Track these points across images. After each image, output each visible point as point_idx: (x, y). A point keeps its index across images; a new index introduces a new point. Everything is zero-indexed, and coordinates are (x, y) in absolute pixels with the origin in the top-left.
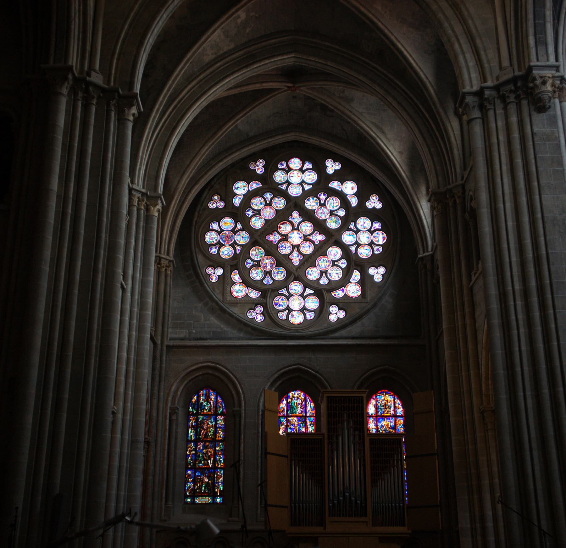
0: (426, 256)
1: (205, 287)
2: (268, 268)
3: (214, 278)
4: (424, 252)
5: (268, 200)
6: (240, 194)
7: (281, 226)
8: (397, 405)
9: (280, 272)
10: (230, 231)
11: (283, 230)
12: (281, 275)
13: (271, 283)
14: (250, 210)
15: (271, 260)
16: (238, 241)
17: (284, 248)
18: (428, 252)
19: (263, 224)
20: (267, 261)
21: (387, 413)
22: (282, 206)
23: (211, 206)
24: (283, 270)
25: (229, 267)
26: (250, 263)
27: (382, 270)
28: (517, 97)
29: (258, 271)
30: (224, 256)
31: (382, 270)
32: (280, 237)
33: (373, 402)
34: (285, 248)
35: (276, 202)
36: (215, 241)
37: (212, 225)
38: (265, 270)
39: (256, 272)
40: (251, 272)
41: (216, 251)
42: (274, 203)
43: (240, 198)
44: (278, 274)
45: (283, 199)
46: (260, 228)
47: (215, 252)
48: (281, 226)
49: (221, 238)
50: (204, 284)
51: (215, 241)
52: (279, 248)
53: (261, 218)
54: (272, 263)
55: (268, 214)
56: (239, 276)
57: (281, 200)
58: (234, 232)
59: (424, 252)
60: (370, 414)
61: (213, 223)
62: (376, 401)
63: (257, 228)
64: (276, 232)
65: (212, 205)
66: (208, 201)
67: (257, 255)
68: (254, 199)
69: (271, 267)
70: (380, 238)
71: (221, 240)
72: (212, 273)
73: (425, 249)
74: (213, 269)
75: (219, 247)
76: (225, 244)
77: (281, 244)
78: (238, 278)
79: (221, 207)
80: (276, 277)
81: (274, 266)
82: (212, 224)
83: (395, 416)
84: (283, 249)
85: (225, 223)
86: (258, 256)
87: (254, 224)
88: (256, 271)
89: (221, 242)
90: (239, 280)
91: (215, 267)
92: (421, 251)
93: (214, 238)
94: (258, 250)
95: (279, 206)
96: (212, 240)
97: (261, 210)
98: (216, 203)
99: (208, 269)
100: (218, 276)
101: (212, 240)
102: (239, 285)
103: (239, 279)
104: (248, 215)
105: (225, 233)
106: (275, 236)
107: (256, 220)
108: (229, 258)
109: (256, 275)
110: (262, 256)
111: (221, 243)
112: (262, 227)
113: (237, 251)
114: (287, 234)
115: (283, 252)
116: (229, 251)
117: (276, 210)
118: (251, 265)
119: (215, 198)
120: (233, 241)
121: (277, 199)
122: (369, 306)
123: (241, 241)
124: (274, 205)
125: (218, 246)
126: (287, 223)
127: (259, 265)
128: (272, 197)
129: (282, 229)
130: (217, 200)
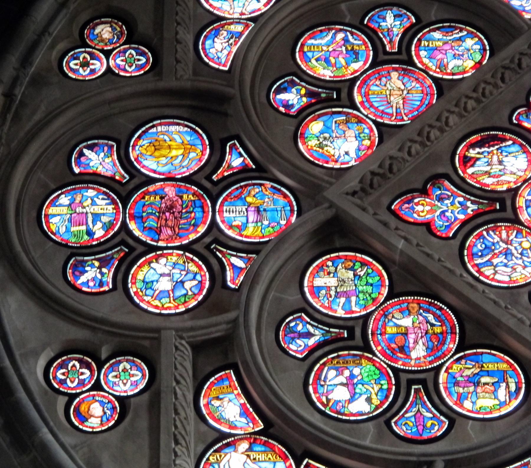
1: (44, 447)
2: (414, 355)
3: (96, 409)
5: (391, 42)
6: (236, 16)
7: (472, 153)
9: (489, 373)
10: (187, 180)
11: (488, 173)
12: (495, 392)
13: (437, 431)
14: (293, 84)
15: (431, 317)
16: (231, 227)
17: (502, 258)
19: (369, 148)
20: (407, 322)
22: (470, 64)
23: (74, 71)
24: (504, 366)
25: (188, 352)
26: (309, 335)
29: (356, 371)
30: (156, 303)
32: (472, 208)
34: (507, 253)
35: (436, 49)
36: (99, 233)
37: (81, 154)
38: (399, 365)
39: (342, 379)
40: (318, 377)
41: (109, 279)
42: (423, 53)
43: (232, 35)
44: (477, 384)
45: (472, 35)
46: (353, 163)
47: (101, 284)
48: (472, 153)
49: (133, 217)
50: (33, 431)
51: (99, 233)
52: (472, 256)
53: (360, 121)
54: (438, 330)
55: (397, 100)
56: (243, 400)
57: (460, 39)
58: (208, 185)
61: (91, 148)
63: (337, 166)
64: (447, 183)
65: (85, 64)
66: (61, 46)
67: (347, 295)
68: (310, 38)
69: (431, 350)
71: (132, 226)
72: (82, 383)
74: (88, 366)
75: (121, 261)
76: (161, 244)
77: (480, 235)
78: (237, 410)
79: (131, 71)
80: (467, 404)
81: (453, 347)
82: (85, 151)
84: (495, 261)
85: (157, 145)
86: (353, 299)
87: (321, 146)
88: (347, 373)
89: (137, 233)
90: (244, 420)
91: (104, 356)
93: (96, 217)
94: (352, 269)
95: (452, 64)
96: (84, 228)
97: (353, 81)
98: (107, 54)
99: (63, 365)
100: (117, 398)
101: (84, 228)
102: (244, 446)
103: (244, 413)
104: (282, 109)
105: (155, 193)
106: (440, 199)
107: (327, 128)
108: (182, 309)
109: (348, 396)
110: (374, 300)
111: (137, 239)
112: (362, 161)
113: (229, 274)
114: (514, 192)
115: (498, 277)
116: (177, 275)
117: (434, 79)
118: (311, 342)
119: (99, 35)
120: (202, 229)
121: (437, 35)
123: (251, 226)
124: (426, 61)
125: (117, 253)
126: (504, 140)
127: (358, 340)
128: (407, 24)
129: (480, 167)
130: (110, 41)
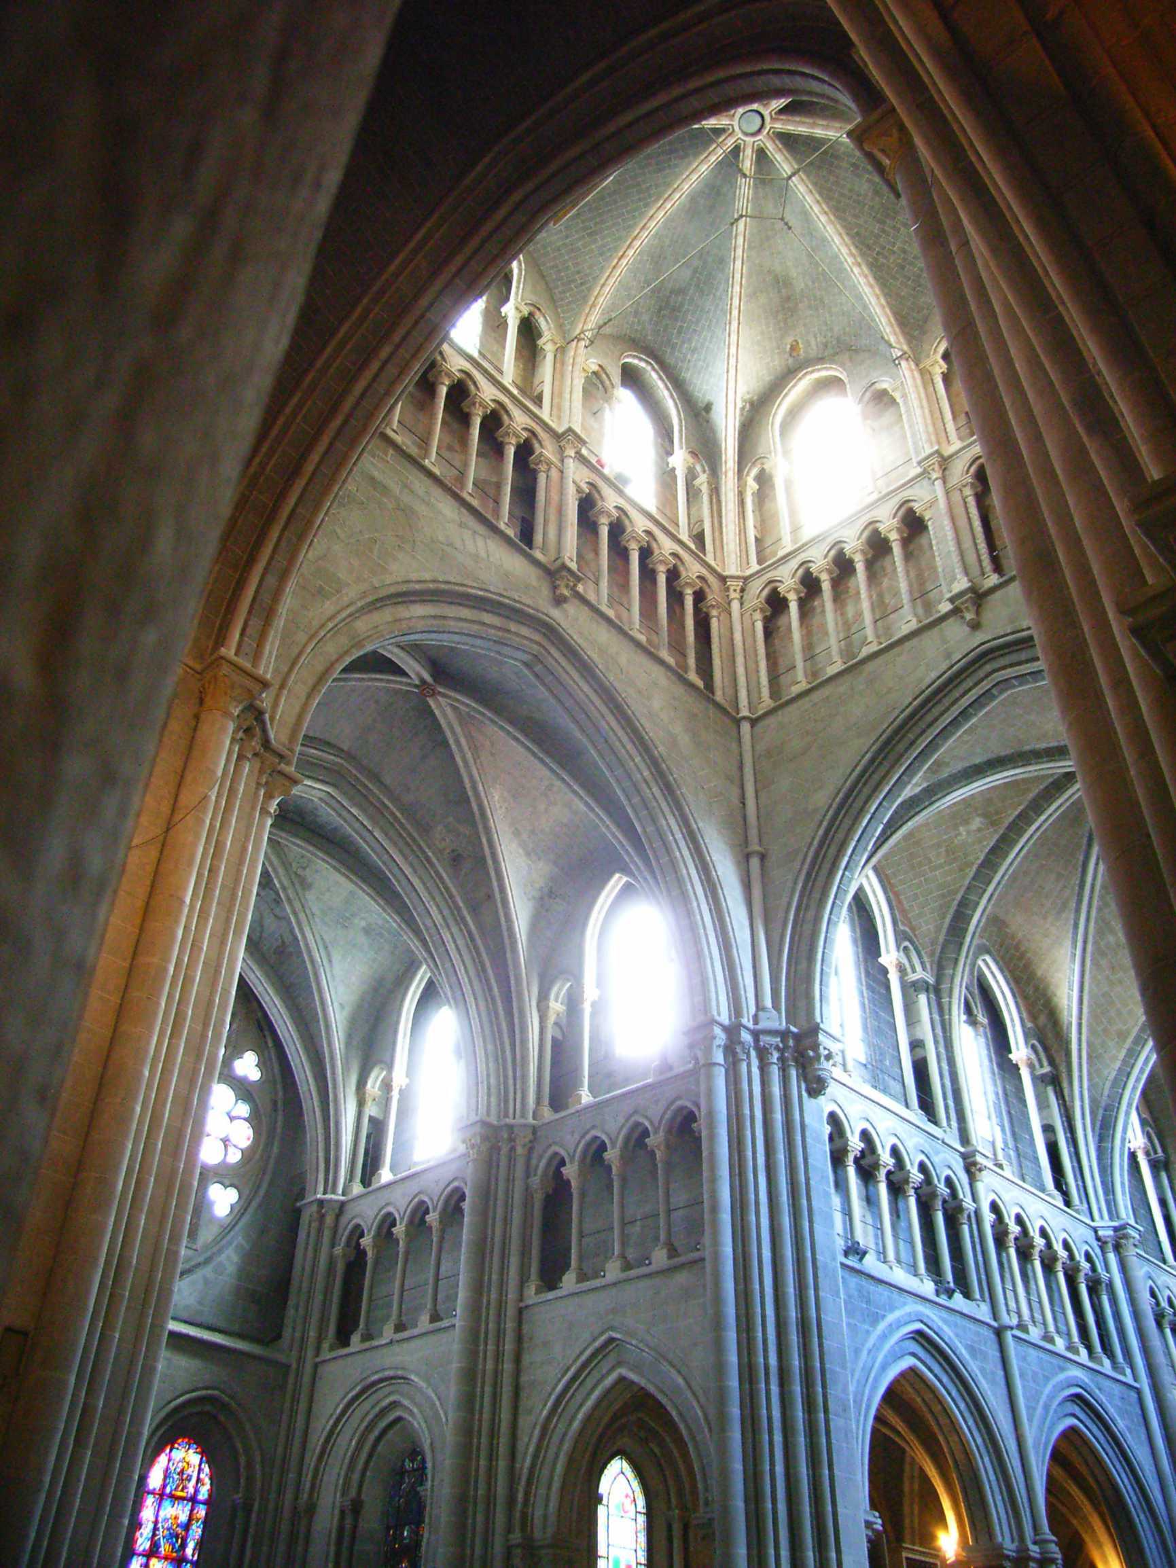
0: (331, 1201)
4: (325, 1193)
8: (202, 1476)
18: (334, 1192)
21: (182, 1490)
27: (232, 1195)
28: (782, 1059)
31: (232, 1195)
33: (163, 1460)
59: (325, 1193)
60: (151, 1487)
62: (169, 1460)
70: (243, 1135)
73: (330, 1186)
83: (193, 1500)
92: (321, 1189)
122: (201, 1259)
